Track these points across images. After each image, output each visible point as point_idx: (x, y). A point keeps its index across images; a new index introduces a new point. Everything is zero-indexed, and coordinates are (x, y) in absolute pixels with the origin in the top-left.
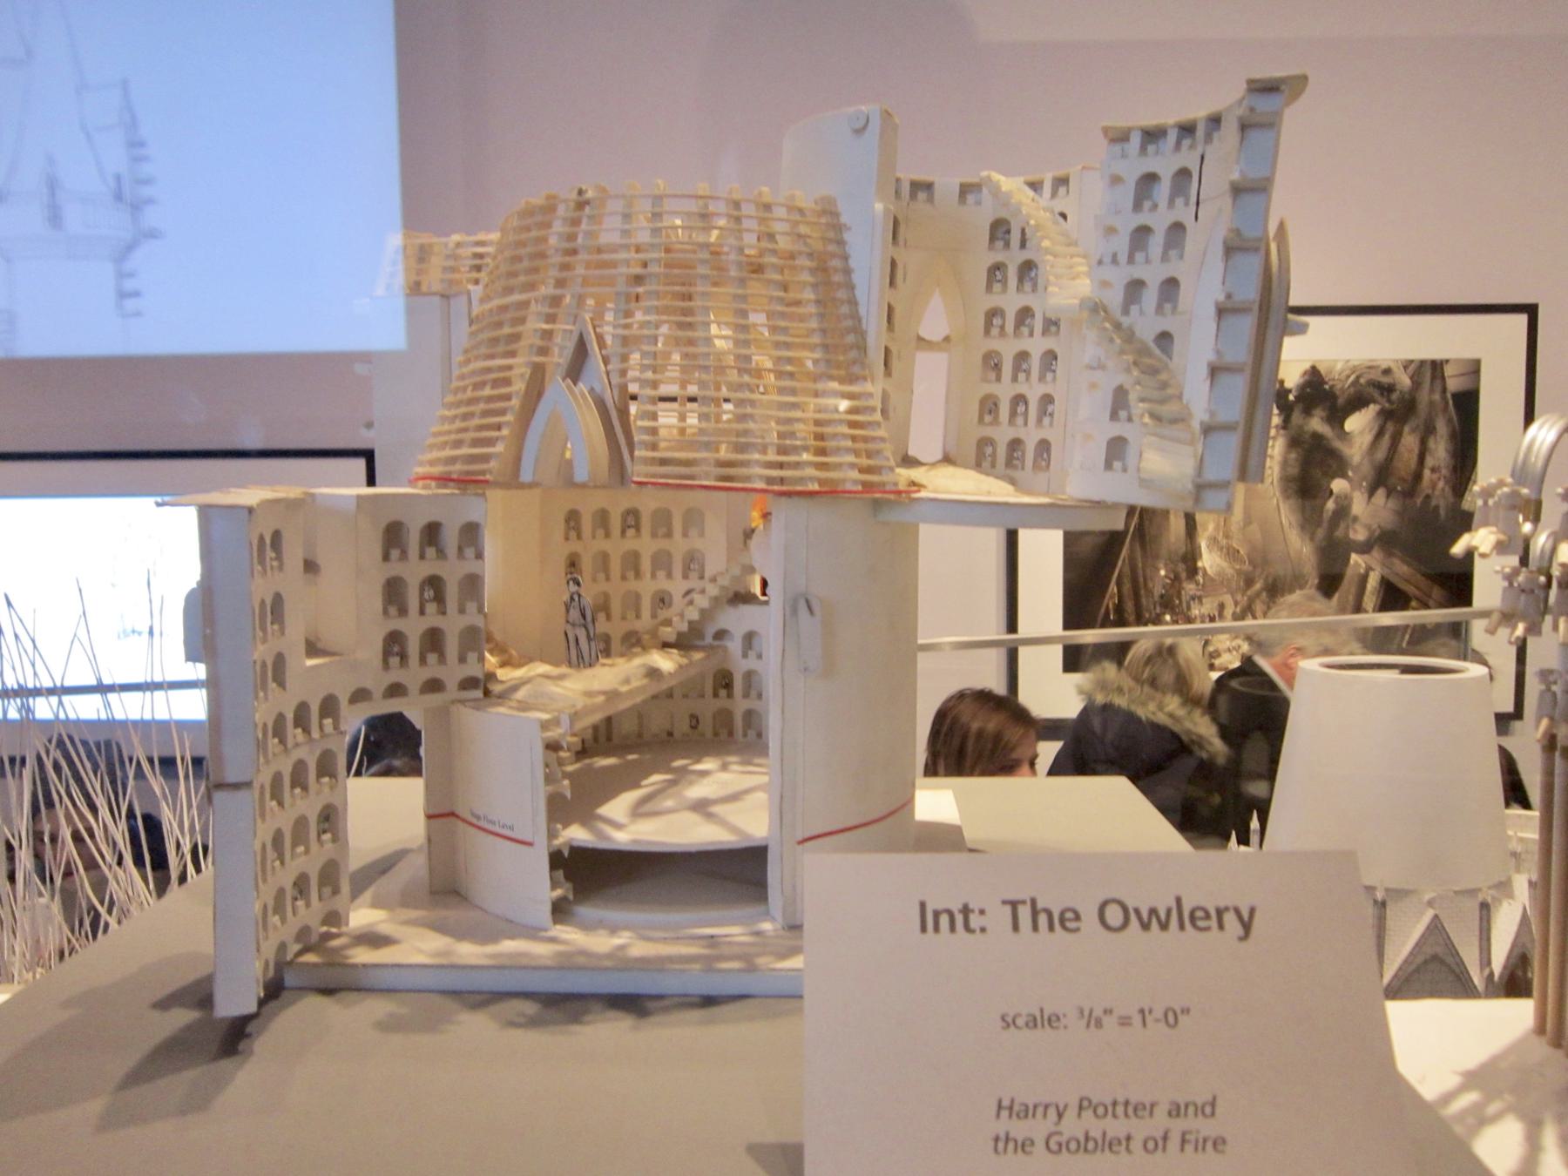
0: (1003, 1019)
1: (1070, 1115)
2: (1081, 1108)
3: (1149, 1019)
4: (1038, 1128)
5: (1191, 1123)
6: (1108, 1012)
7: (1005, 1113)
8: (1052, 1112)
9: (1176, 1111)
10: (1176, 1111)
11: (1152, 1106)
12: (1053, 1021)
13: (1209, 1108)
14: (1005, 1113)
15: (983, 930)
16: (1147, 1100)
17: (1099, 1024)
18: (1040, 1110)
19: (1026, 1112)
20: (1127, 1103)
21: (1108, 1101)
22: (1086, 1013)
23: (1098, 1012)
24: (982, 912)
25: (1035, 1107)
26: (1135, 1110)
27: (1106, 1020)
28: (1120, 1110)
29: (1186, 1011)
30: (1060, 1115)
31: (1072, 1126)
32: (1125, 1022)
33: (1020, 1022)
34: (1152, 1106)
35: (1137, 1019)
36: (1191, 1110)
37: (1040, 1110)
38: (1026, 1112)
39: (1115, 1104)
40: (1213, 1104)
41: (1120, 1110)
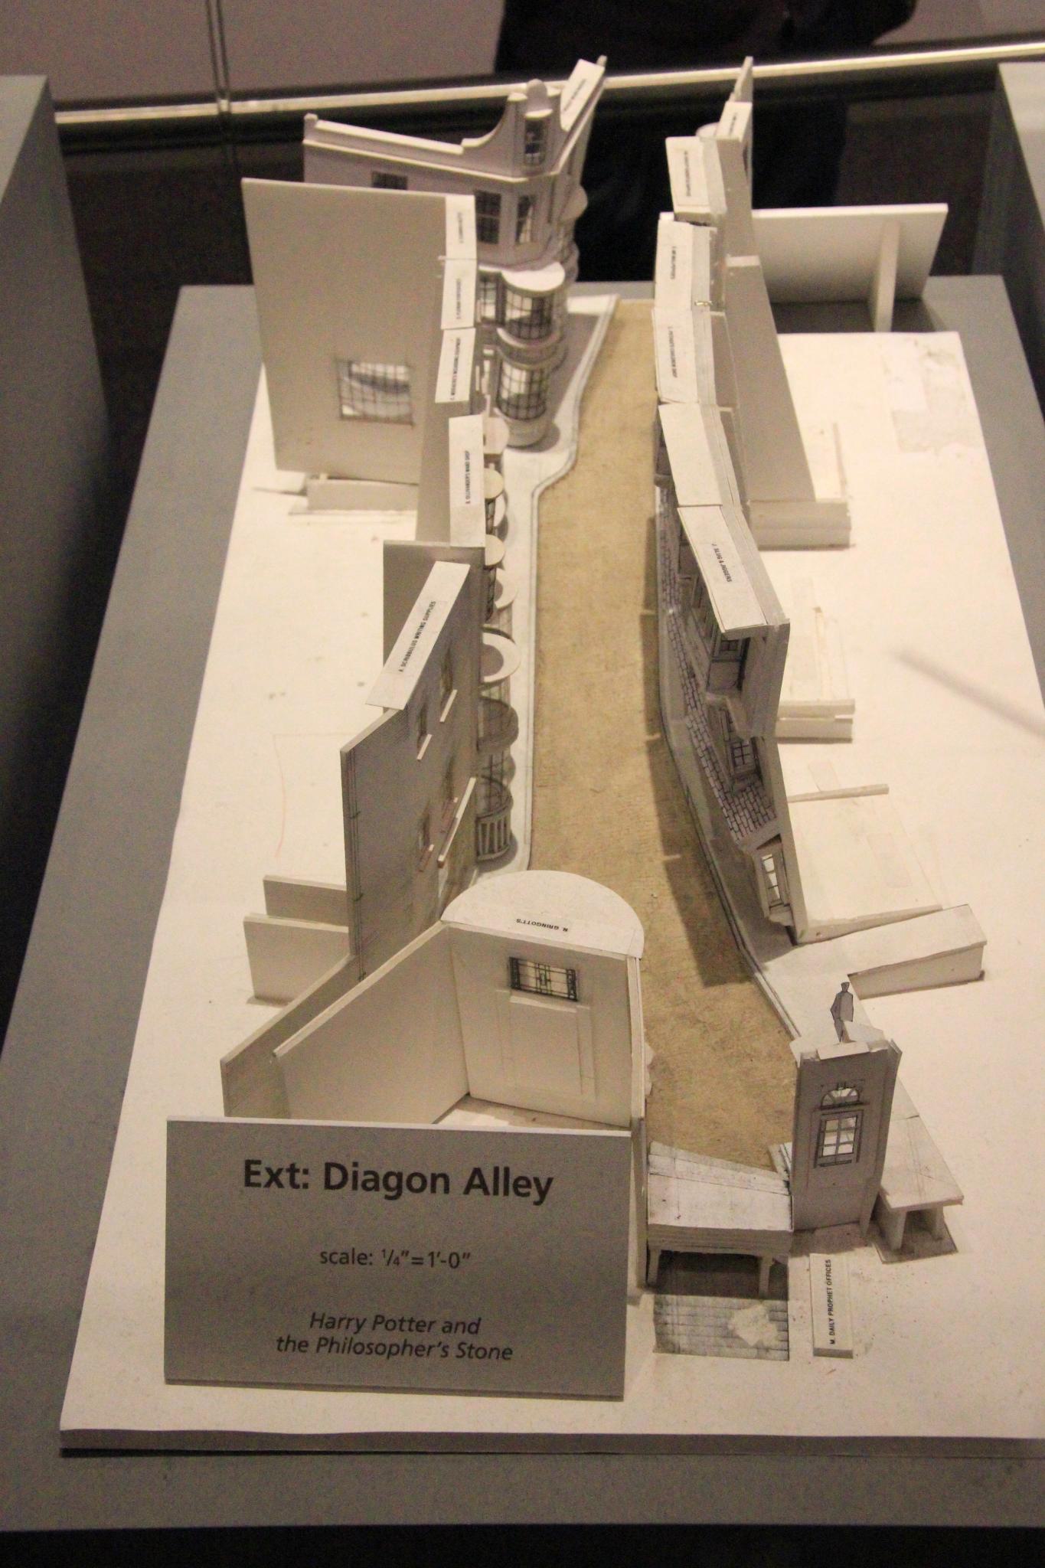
0: (322, 1254)
1: (367, 1327)
2: (376, 1322)
3: (437, 1261)
4: (339, 1334)
5: (461, 1336)
6: (406, 1253)
7: (317, 1324)
8: (353, 1323)
9: (449, 1327)
10: (449, 1327)
11: (431, 1323)
12: (362, 1259)
13: (474, 1327)
14: (317, 1324)
15: (306, 1186)
16: (428, 1320)
17: (397, 1262)
18: (345, 1322)
19: (332, 1324)
20: (411, 1321)
21: (397, 1317)
22: (388, 1254)
23: (397, 1253)
24: (306, 1172)
25: (341, 1320)
26: (418, 1326)
27: (402, 1260)
28: (406, 1326)
29: (467, 1255)
30: (359, 1327)
31: (365, 1336)
32: (417, 1261)
33: (335, 1258)
34: (431, 1323)
35: (427, 1259)
36: (461, 1327)
37: (345, 1322)
38: (332, 1324)
39: (402, 1321)
40: (478, 1325)
41: (406, 1326)
